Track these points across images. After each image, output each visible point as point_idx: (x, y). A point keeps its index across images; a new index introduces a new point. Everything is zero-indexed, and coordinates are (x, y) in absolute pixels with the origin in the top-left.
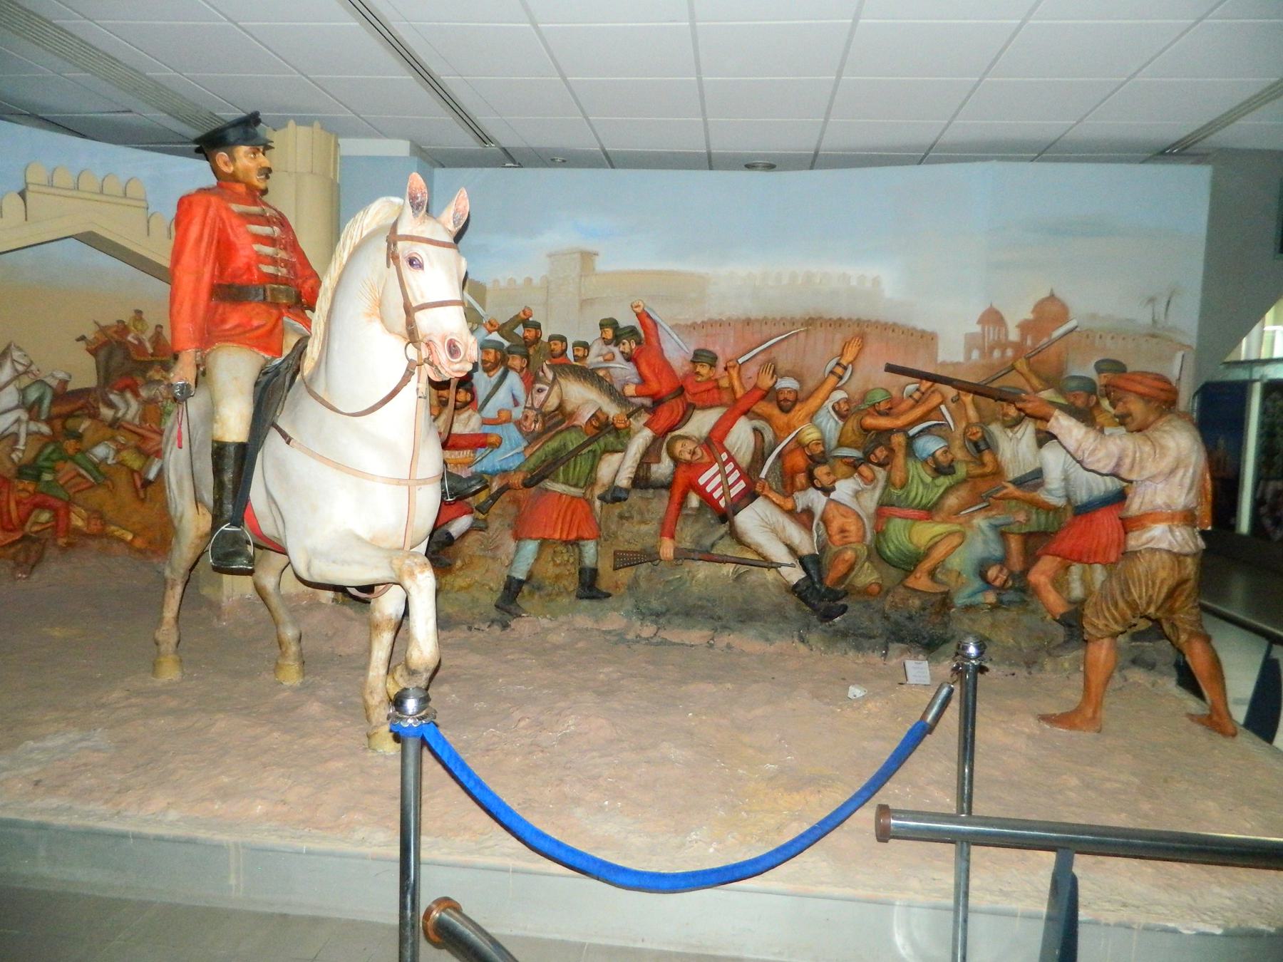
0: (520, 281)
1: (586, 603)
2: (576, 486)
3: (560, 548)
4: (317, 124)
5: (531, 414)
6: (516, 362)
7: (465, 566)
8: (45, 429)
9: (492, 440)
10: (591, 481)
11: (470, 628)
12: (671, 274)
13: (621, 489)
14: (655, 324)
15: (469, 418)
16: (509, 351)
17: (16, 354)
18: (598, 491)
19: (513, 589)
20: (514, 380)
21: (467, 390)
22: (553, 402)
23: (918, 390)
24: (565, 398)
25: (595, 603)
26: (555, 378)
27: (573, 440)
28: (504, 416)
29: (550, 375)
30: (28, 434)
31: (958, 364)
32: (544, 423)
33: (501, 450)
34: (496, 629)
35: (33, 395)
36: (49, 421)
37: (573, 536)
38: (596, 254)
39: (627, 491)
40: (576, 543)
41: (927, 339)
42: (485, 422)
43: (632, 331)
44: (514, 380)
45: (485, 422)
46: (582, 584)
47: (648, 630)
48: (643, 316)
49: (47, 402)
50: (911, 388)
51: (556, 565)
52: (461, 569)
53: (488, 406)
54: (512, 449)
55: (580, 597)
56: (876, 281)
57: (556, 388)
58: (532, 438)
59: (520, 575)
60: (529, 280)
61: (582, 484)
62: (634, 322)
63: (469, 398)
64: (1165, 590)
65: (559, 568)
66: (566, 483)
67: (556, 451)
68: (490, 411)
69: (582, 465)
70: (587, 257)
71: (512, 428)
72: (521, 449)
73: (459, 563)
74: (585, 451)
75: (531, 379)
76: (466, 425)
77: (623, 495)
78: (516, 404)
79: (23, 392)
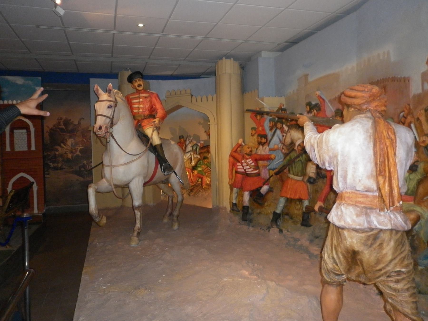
0: (292, 93)
1: (303, 227)
2: (297, 175)
3: (298, 203)
4: (224, 58)
5: (282, 146)
6: (279, 125)
7: (269, 206)
8: (199, 157)
9: (273, 156)
10: (303, 173)
11: (261, 229)
12: (328, 76)
13: (310, 178)
14: (324, 100)
15: (266, 148)
16: (277, 122)
17: (189, 137)
18: (306, 179)
19: (276, 217)
20: (278, 132)
21: (265, 138)
22: (288, 141)
23: (404, 116)
24: (293, 138)
25: (305, 228)
26: (288, 130)
27: (293, 155)
28: (276, 147)
29: (286, 128)
30: (194, 158)
31: (419, 96)
32: (288, 150)
33: (275, 160)
34: (267, 231)
35: (195, 148)
36: (200, 154)
37: (297, 197)
38: (308, 75)
39: (314, 180)
40: (300, 200)
41: (406, 81)
42: (271, 150)
43: (316, 105)
44: (278, 132)
45: (271, 150)
46: (303, 220)
47: (307, 243)
48: (320, 97)
49: (198, 149)
50: (402, 114)
51: (297, 210)
52: (267, 205)
53: (271, 143)
54: (279, 160)
55: (302, 225)
56: (388, 53)
57: (288, 134)
58: (286, 155)
59: (278, 211)
60: (294, 91)
61: (299, 174)
62: (318, 102)
63: (265, 141)
64: (341, 256)
65: (297, 211)
66: (293, 174)
67: (289, 161)
68: (272, 145)
69: (298, 167)
70: (306, 76)
71: (280, 152)
72: (282, 160)
73: (266, 204)
74: (297, 160)
75: (283, 131)
76: (265, 151)
77: (312, 181)
78: (280, 141)
79: (192, 147)
